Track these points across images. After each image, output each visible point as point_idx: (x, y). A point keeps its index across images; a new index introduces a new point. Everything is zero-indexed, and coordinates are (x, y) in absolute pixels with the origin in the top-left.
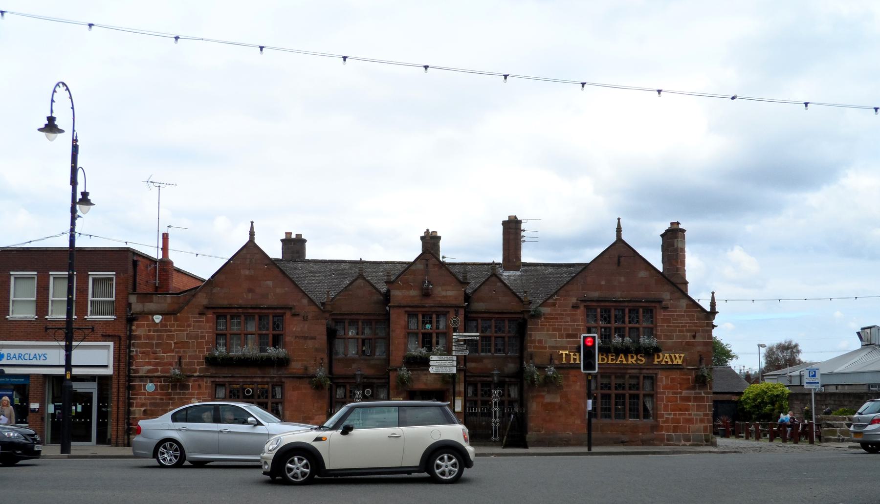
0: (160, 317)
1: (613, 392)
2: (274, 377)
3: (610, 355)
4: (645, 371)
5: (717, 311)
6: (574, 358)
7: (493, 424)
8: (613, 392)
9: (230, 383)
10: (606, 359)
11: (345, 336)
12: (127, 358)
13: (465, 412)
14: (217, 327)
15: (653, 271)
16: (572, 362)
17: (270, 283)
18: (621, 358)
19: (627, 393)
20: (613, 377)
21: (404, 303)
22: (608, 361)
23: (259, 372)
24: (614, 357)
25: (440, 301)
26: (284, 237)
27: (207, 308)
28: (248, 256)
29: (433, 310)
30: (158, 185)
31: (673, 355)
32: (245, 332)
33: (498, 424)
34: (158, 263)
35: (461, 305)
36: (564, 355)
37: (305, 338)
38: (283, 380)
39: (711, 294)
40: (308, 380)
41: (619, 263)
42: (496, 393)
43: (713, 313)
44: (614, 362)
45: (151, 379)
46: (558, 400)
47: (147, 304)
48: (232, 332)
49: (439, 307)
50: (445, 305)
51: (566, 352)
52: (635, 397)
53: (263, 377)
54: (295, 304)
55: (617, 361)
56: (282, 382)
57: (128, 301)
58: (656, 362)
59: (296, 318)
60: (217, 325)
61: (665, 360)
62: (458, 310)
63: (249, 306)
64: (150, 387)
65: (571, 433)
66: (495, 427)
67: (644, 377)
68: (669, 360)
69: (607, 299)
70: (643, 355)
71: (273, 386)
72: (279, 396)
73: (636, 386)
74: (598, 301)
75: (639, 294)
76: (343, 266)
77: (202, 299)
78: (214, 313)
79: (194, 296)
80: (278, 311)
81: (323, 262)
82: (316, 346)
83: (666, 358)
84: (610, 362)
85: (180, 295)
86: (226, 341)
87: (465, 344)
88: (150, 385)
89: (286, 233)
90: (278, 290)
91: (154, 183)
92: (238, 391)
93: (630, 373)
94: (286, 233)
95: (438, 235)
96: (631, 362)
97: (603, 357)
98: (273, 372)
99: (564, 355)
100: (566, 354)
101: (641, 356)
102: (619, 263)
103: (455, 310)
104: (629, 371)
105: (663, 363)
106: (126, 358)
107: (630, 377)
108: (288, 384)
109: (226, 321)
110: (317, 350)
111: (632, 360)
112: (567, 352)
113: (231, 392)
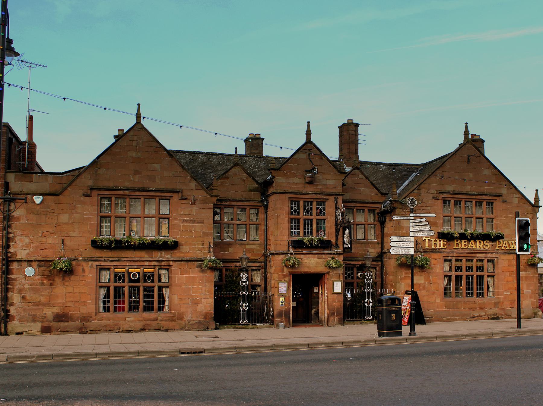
0: (41, 198)
1: (464, 273)
2: (162, 260)
3: (463, 241)
4: (489, 255)
5: (540, 205)
6: (435, 243)
7: (366, 304)
8: (464, 273)
9: (116, 267)
10: (459, 244)
11: (221, 221)
12: (4, 241)
13: (343, 293)
14: (101, 209)
15: (493, 170)
16: (433, 247)
17: (157, 166)
18: (472, 244)
19: (475, 274)
20: (464, 260)
21: (288, 190)
22: (461, 246)
23: (146, 256)
24: (466, 243)
25: (321, 189)
26: (116, 133)
27: (92, 189)
28: (135, 138)
29: (315, 197)
30: (28, 65)
31: (510, 242)
32: (131, 215)
33: (371, 305)
34: (27, 143)
35: (340, 194)
36: (427, 241)
37: (194, 222)
38: (171, 263)
39: (536, 191)
40: (196, 263)
41: (469, 161)
42: (368, 275)
43: (536, 206)
44: (466, 247)
45: (29, 263)
46: (422, 282)
47: (26, 183)
48: (117, 215)
49: (320, 194)
50: (326, 193)
51: (429, 238)
52: (481, 278)
53: (150, 261)
54: (182, 188)
55: (468, 247)
56: (170, 266)
57: (5, 179)
58: (497, 248)
59: (184, 202)
60: (101, 207)
61: (504, 245)
62: (337, 198)
63: (136, 189)
64: (30, 271)
65: (433, 311)
66: (369, 307)
67: (488, 261)
68: (507, 245)
69: (461, 192)
70: (488, 241)
71: (159, 269)
72: (164, 279)
73: (480, 269)
74: (453, 193)
75: (484, 189)
76: (201, 157)
77: (87, 181)
78: (98, 194)
79: (78, 176)
80: (165, 194)
81: (181, 153)
82: (204, 230)
83: (505, 244)
84: (463, 247)
85: (62, 176)
86: (111, 224)
87: (428, 225)
88: (30, 269)
89: (119, 130)
90: (165, 174)
91: (24, 62)
92: (124, 276)
93: (478, 257)
94: (119, 130)
95: (261, 137)
96: (479, 247)
97: (457, 243)
98: (165, 255)
99: (427, 241)
100: (429, 240)
101: (486, 242)
102: (469, 161)
103: (335, 198)
104: (478, 255)
105: (503, 248)
106: (3, 241)
107: (477, 261)
108: (175, 267)
109: (111, 203)
110: (205, 234)
111: (480, 246)
112: (429, 238)
113: (116, 275)
